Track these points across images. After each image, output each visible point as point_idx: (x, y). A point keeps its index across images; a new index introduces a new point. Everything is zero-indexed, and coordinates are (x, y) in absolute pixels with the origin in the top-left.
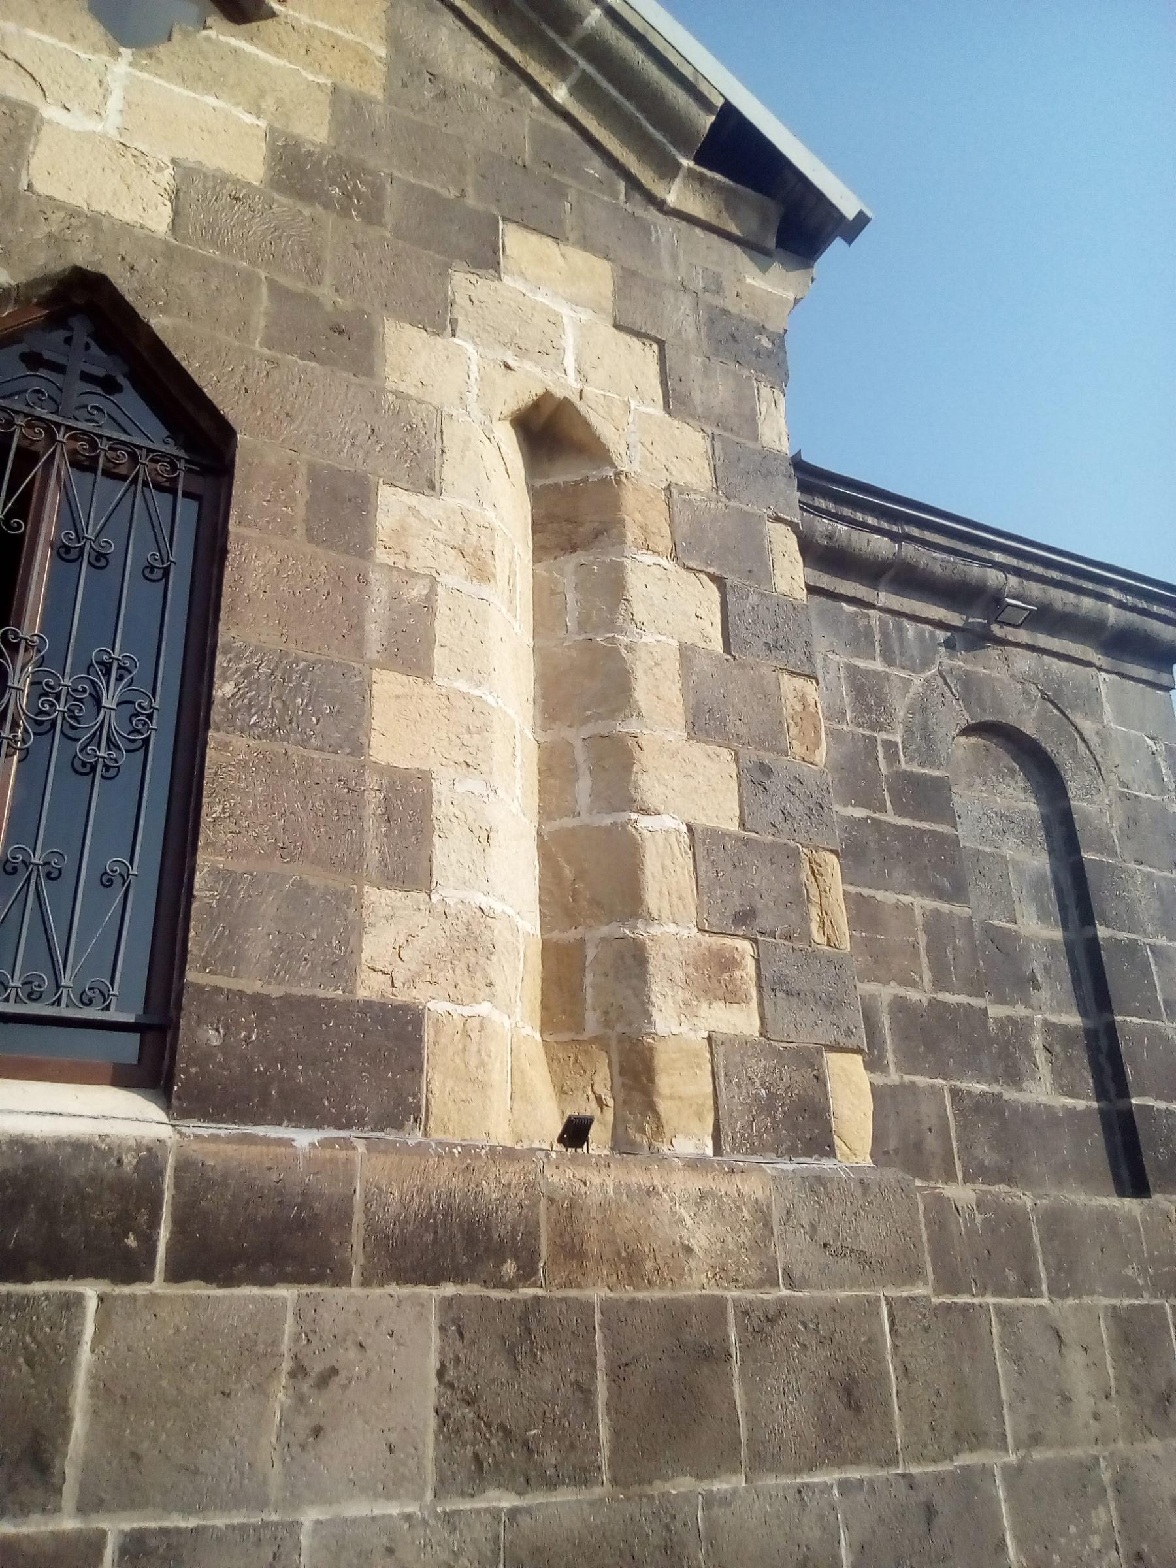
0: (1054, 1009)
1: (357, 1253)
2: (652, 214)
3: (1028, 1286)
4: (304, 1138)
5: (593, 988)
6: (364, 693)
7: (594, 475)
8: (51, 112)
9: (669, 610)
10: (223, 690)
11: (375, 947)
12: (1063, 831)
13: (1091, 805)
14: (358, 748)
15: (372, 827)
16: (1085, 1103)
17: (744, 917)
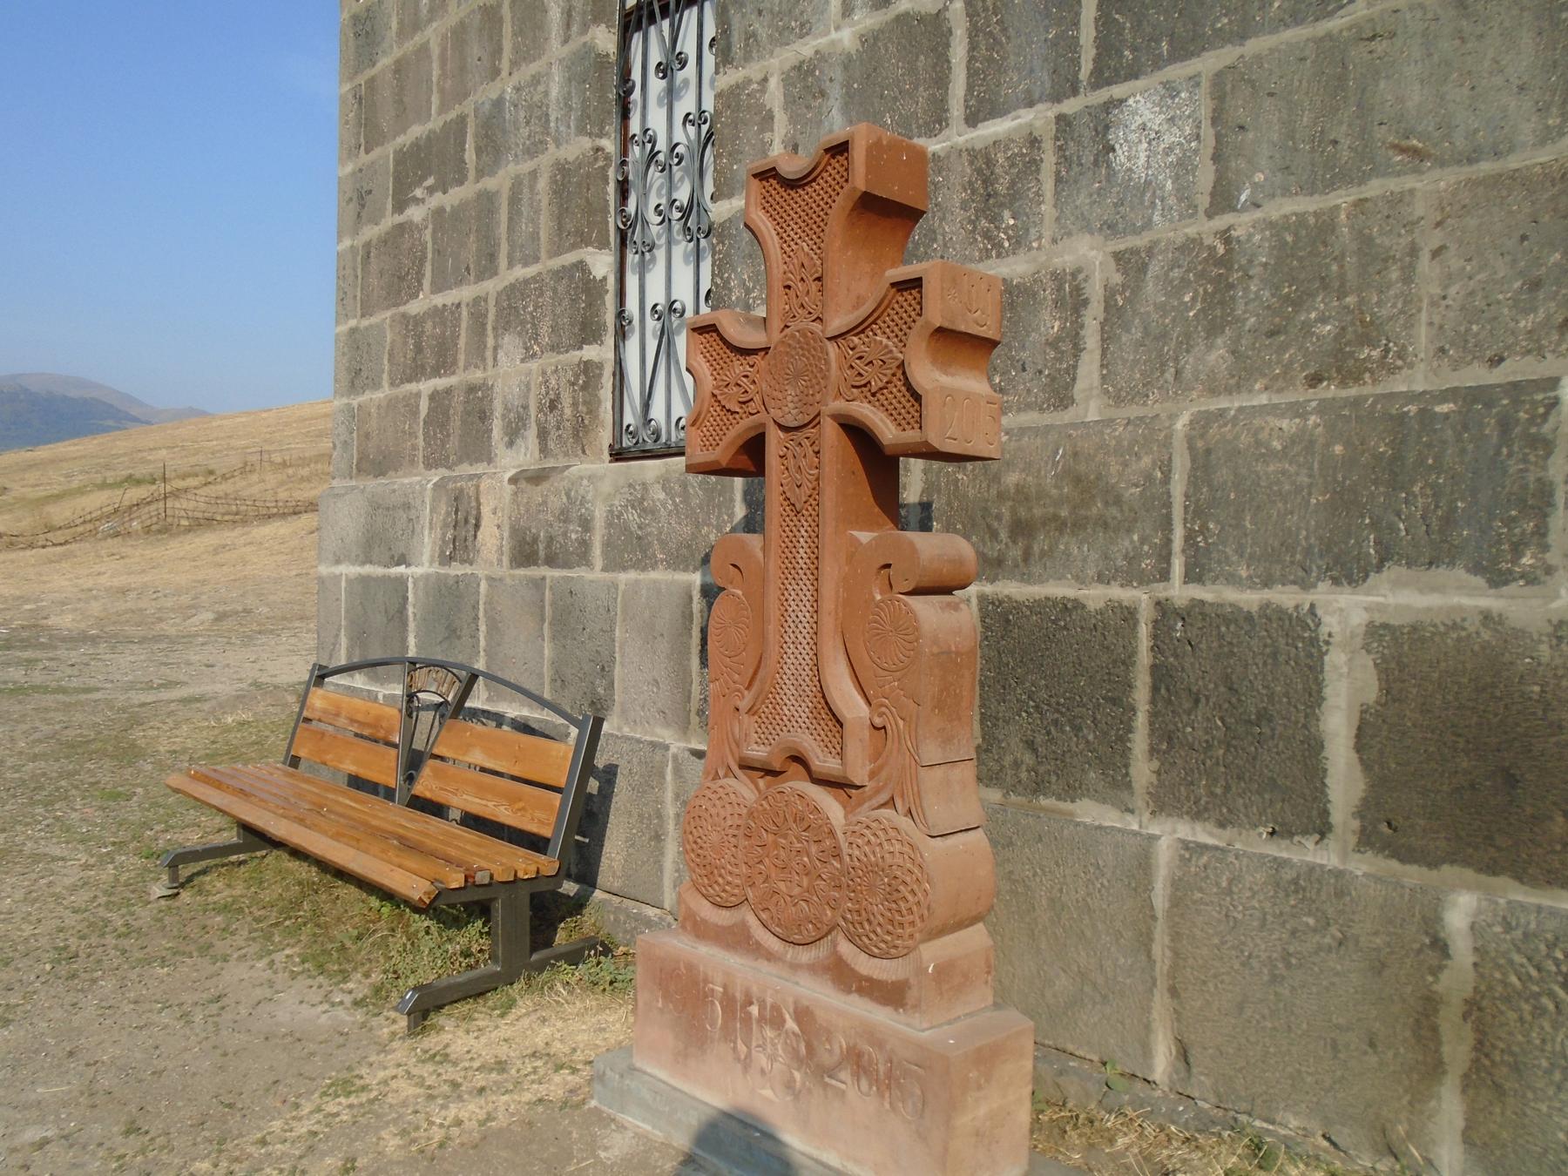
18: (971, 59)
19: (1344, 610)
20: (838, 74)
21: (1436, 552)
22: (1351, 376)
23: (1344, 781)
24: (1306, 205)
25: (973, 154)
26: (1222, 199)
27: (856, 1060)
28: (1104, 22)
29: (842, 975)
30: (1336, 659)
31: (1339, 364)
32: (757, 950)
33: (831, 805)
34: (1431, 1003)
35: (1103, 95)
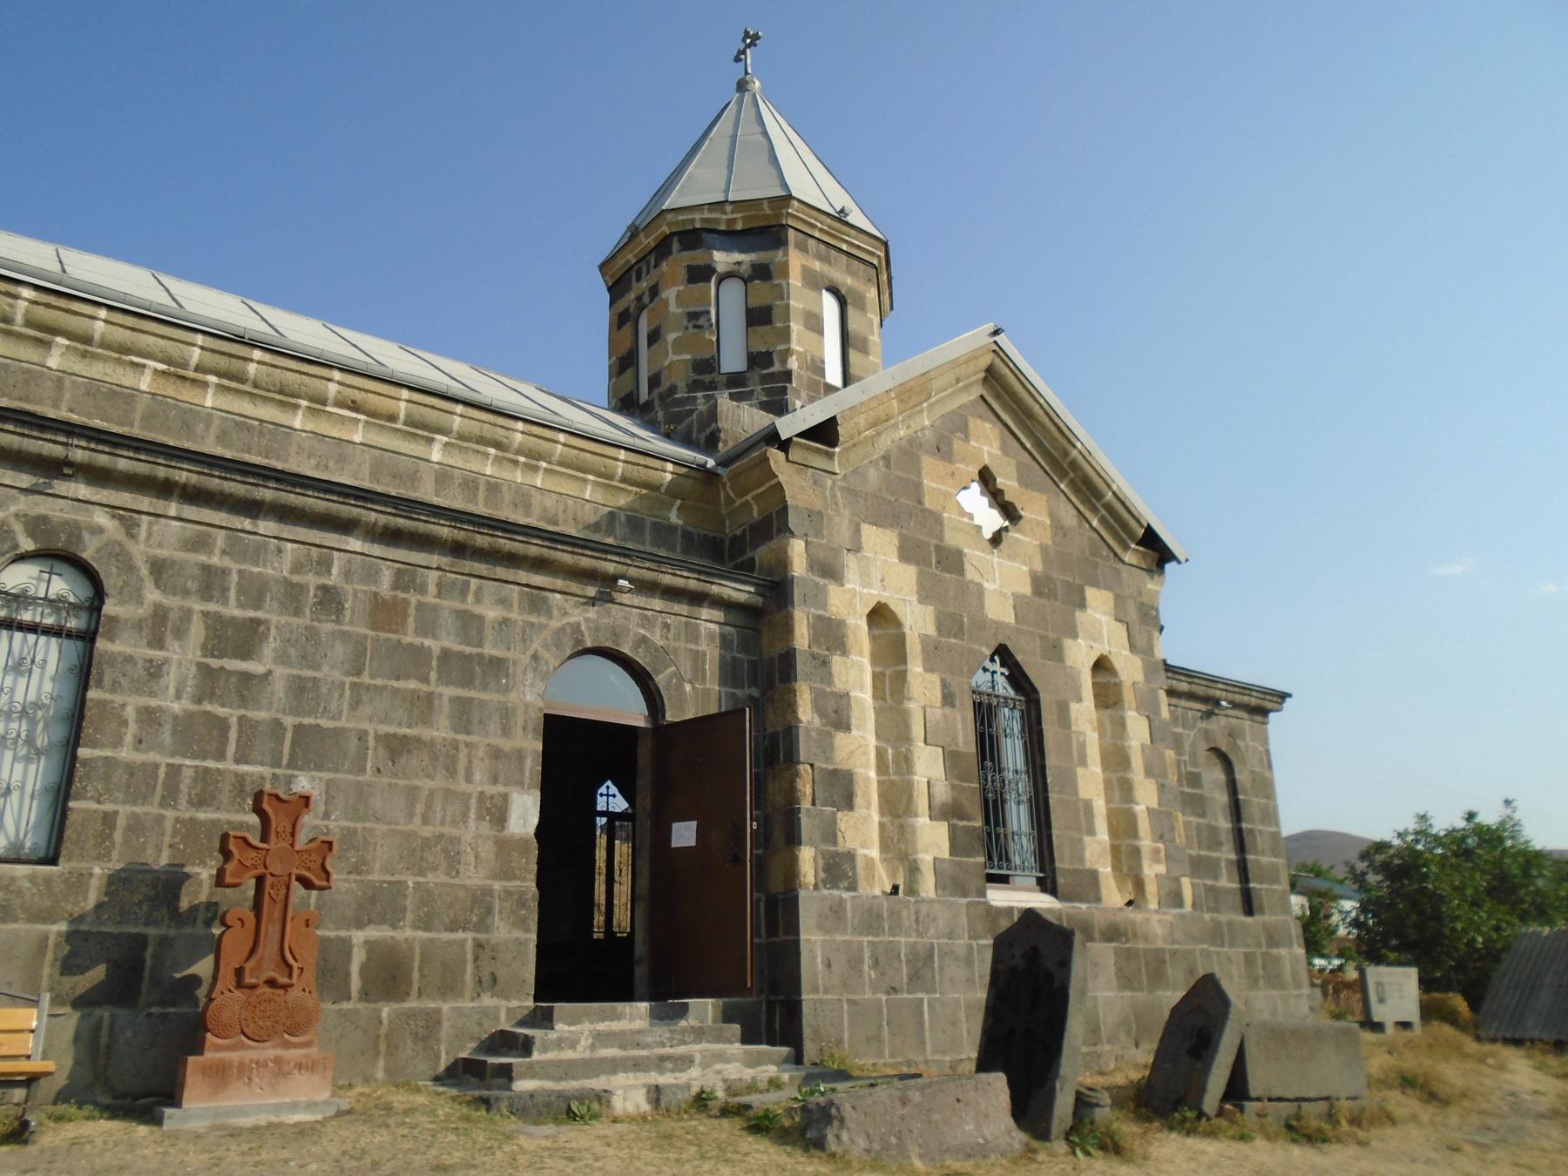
0: (1228, 854)
1: (1097, 935)
2: (1120, 566)
3: (1222, 945)
4: (1084, 906)
5: (1126, 859)
6: (1075, 774)
7: (1113, 680)
8: (986, 585)
9: (1137, 729)
10: (1049, 780)
11: (1087, 854)
12: (1232, 787)
13: (1241, 776)
14: (1076, 794)
15: (1083, 818)
16: (1236, 885)
17: (1161, 837)
18: (238, 741)
19: (358, 937)
20: (171, 720)
21: (381, 920)
22: (360, 873)
23: (355, 983)
24: (350, 824)
25: (236, 774)
26: (326, 816)
27: (299, 1066)
28: (292, 749)
29: (288, 1045)
30: (355, 950)
31: (356, 869)
32: (249, 1047)
33: (281, 992)
34: (378, 1037)
35: (290, 772)
